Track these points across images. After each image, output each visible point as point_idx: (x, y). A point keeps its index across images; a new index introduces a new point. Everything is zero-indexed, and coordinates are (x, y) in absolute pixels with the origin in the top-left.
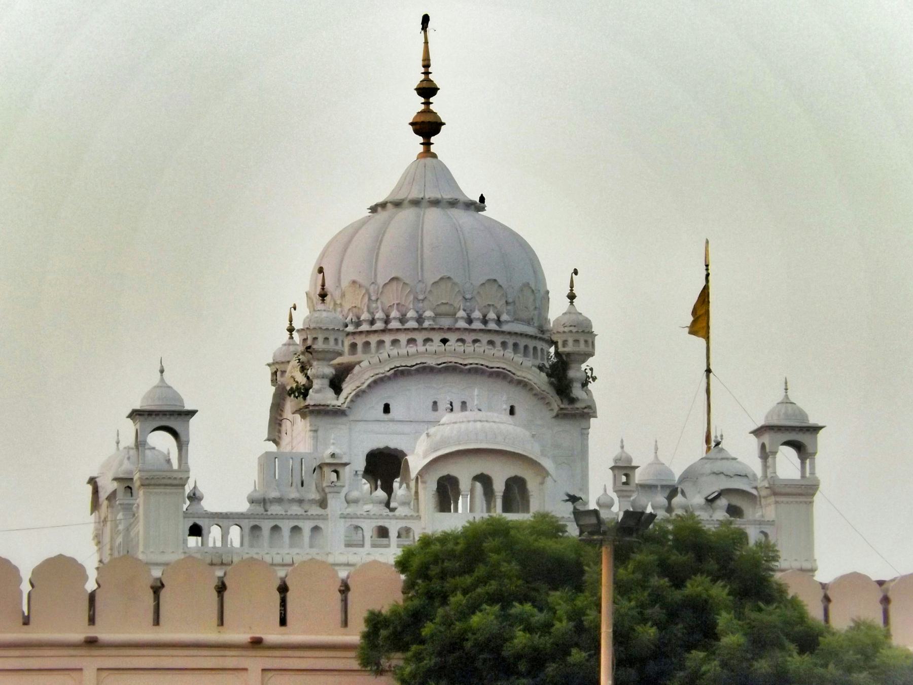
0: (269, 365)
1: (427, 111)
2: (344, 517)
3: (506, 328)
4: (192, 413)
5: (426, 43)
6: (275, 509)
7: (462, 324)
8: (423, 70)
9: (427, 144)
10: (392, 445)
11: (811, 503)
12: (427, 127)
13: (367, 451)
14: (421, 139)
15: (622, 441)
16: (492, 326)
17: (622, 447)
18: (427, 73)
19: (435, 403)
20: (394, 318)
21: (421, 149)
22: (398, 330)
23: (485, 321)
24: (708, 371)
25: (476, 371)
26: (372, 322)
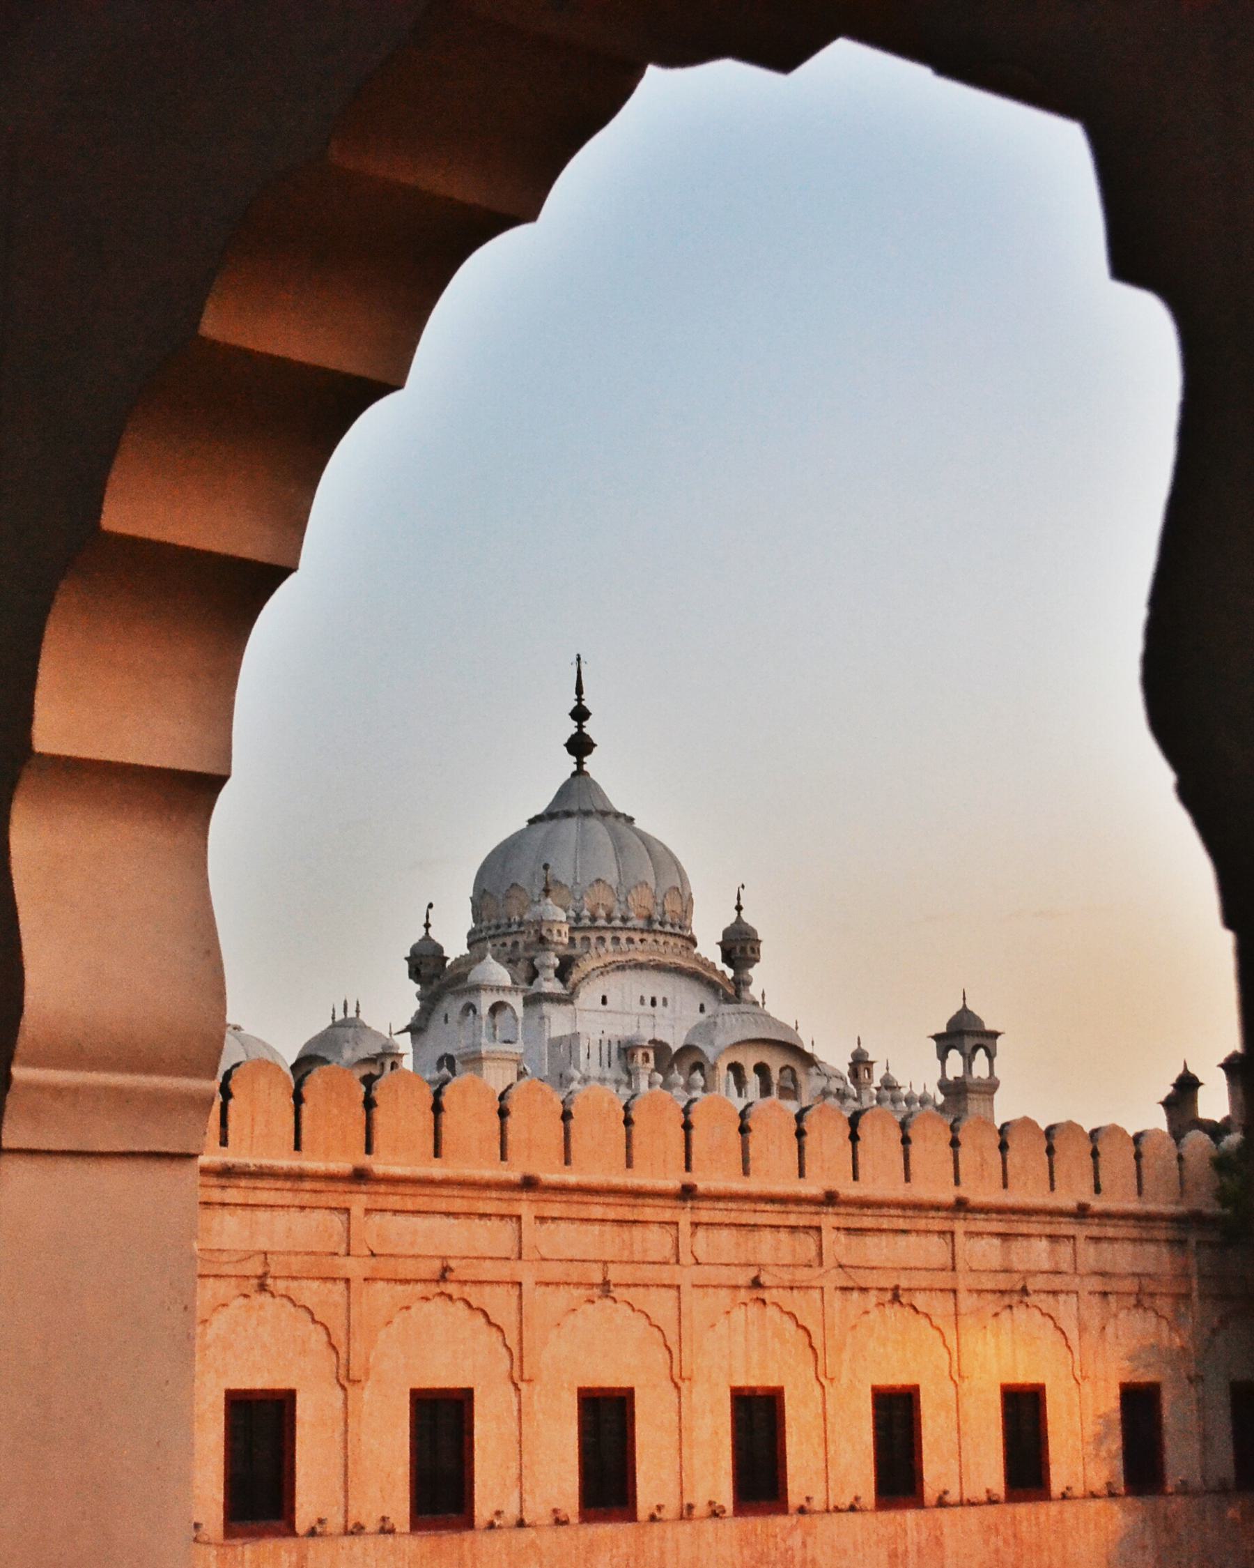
5: (579, 672)
9: (580, 763)
11: (991, 1100)
14: (574, 759)
18: (580, 700)
21: (575, 768)
22: (604, 928)
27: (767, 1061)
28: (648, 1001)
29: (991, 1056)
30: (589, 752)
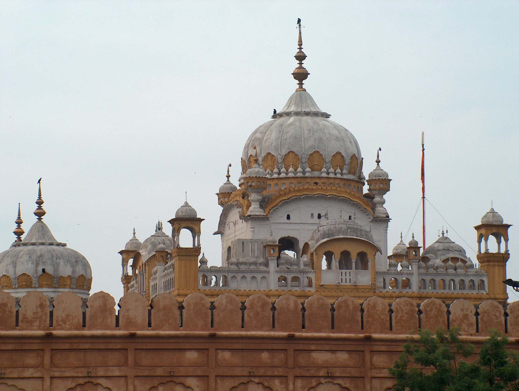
0: (217, 194)
1: (301, 67)
2: (277, 272)
3: (345, 177)
4: (201, 220)
5: (300, 33)
6: (243, 267)
7: (324, 175)
8: (298, 47)
9: (301, 84)
10: (291, 236)
12: (301, 76)
13: (279, 238)
14: (297, 82)
15: (413, 234)
16: (339, 176)
17: (413, 237)
18: (300, 48)
19: (312, 214)
20: (291, 172)
21: (298, 86)
24: (423, 197)
25: (335, 199)
26: (279, 173)
27: (348, 249)
28: (316, 216)
29: (507, 240)
30: (306, 78)
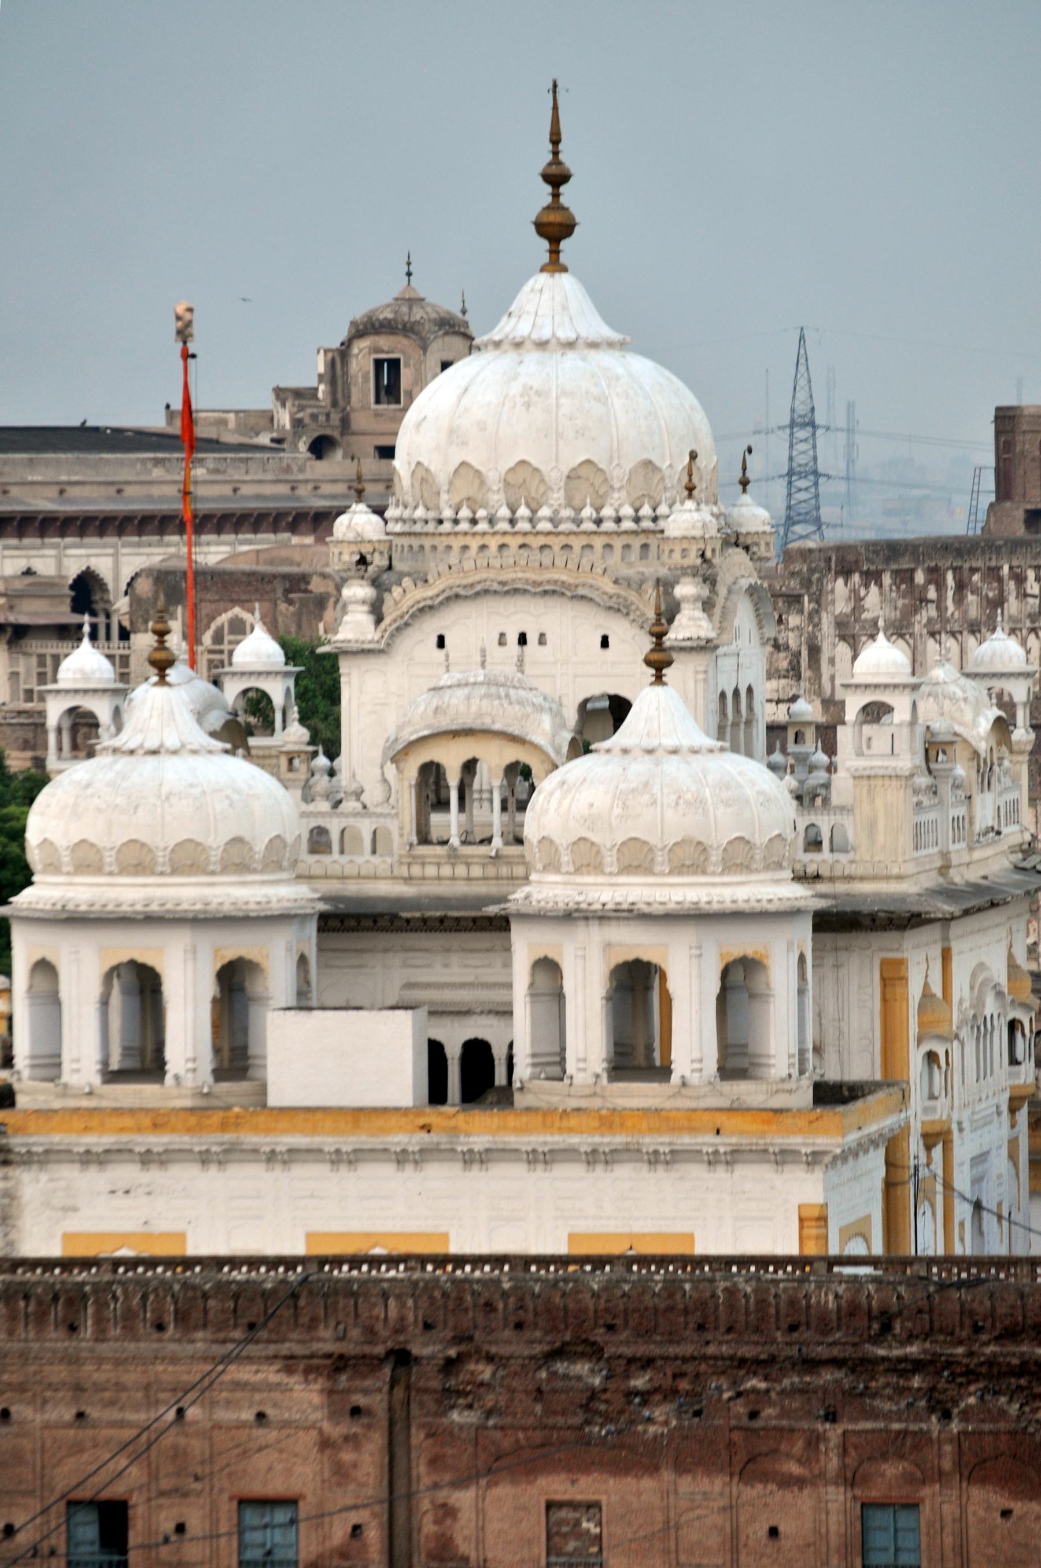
1: (556, 205)
5: (555, 108)
9: (555, 252)
18: (556, 153)
21: (546, 258)
23: (637, 520)
